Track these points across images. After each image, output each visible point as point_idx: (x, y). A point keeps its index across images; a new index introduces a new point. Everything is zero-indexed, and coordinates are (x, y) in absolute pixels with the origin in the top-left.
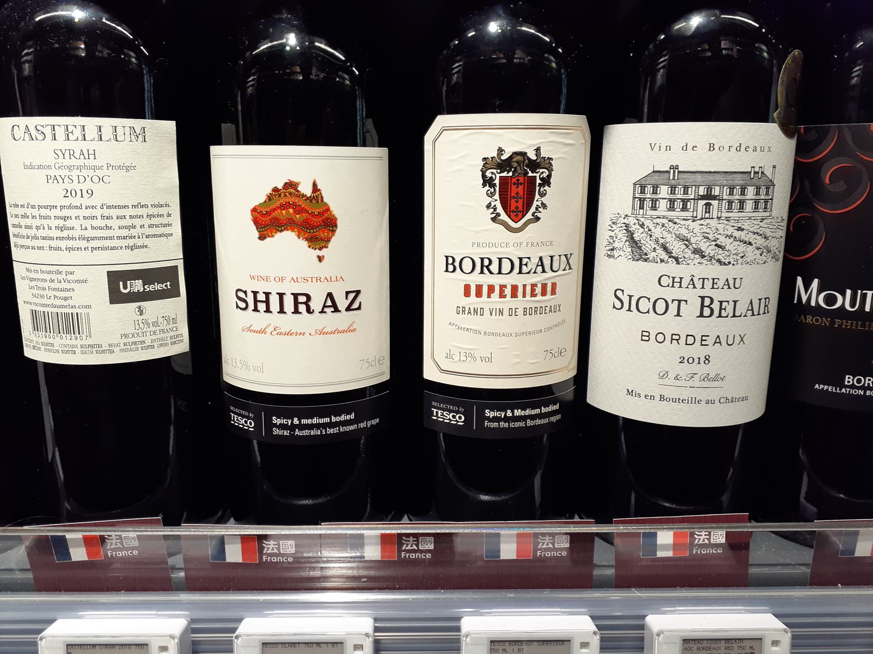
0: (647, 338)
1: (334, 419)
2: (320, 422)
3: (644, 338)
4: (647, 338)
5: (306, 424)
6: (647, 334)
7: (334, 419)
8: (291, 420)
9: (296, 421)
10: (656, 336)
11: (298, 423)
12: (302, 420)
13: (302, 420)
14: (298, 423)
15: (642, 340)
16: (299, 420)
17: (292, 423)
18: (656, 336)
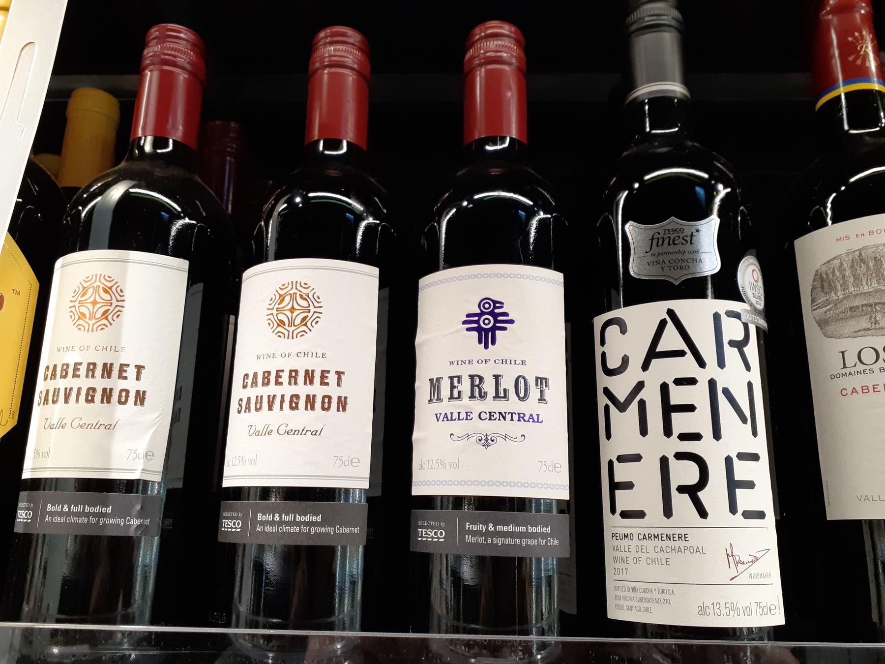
0: (867, 391)
1: (298, 518)
2: (474, 529)
3: (864, 391)
4: (867, 391)
5: (522, 532)
6: (866, 388)
7: (298, 518)
8: (485, 526)
9: (491, 527)
10: (841, 391)
11: (493, 529)
12: (498, 527)
13: (498, 527)
14: (493, 529)
15: (863, 393)
16: (495, 526)
17: (487, 529)
18: (841, 391)
